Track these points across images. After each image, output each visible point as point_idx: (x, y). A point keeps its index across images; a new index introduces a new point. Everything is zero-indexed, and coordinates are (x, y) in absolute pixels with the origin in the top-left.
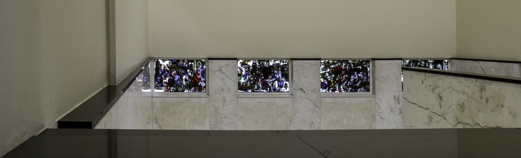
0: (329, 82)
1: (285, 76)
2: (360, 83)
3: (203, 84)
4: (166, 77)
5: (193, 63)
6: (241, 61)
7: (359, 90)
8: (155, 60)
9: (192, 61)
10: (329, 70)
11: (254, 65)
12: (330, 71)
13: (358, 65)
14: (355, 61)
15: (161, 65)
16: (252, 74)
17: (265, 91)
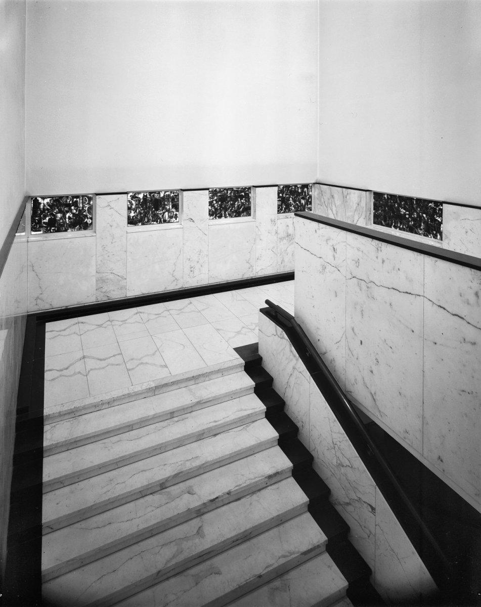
0: (216, 209)
1: (176, 207)
3: (89, 221)
4: (45, 217)
5: (78, 199)
6: (131, 194)
8: (32, 199)
9: (77, 197)
10: (216, 198)
11: (145, 197)
13: (242, 192)
14: (239, 188)
15: (40, 203)
16: (142, 207)
17: (155, 223)
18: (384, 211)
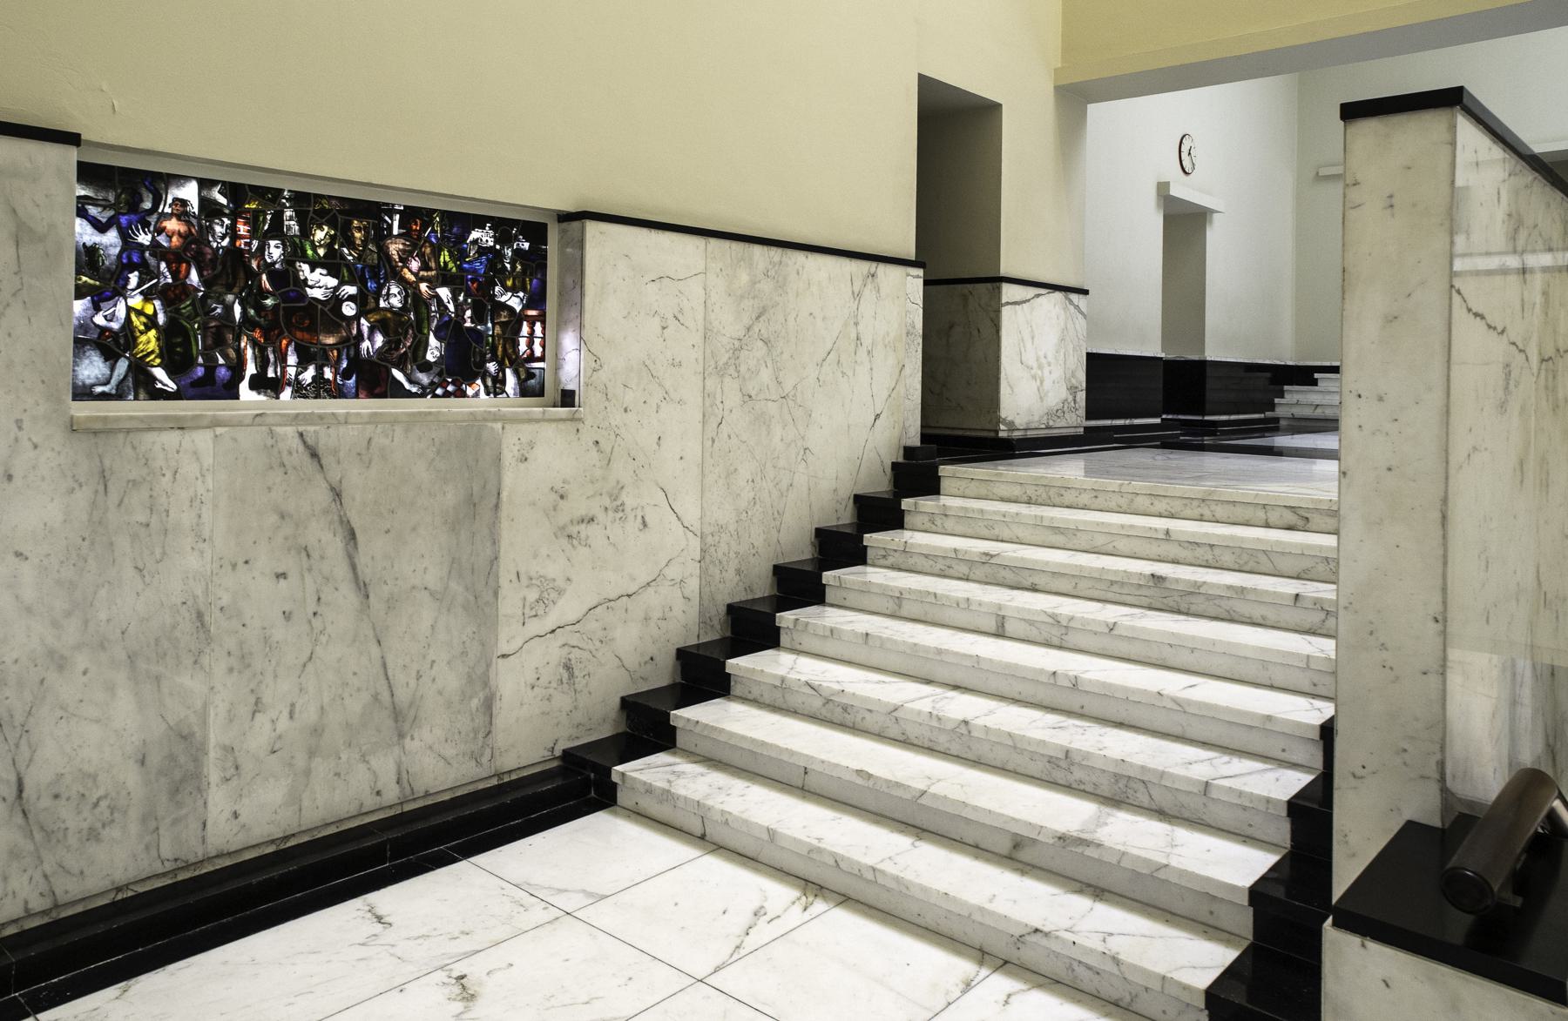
18: (172, 296)
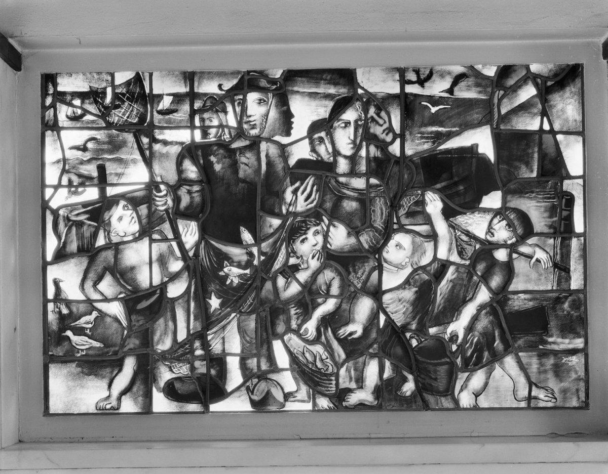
2: (481, 308)
7: (478, 380)
12: (153, 185)
